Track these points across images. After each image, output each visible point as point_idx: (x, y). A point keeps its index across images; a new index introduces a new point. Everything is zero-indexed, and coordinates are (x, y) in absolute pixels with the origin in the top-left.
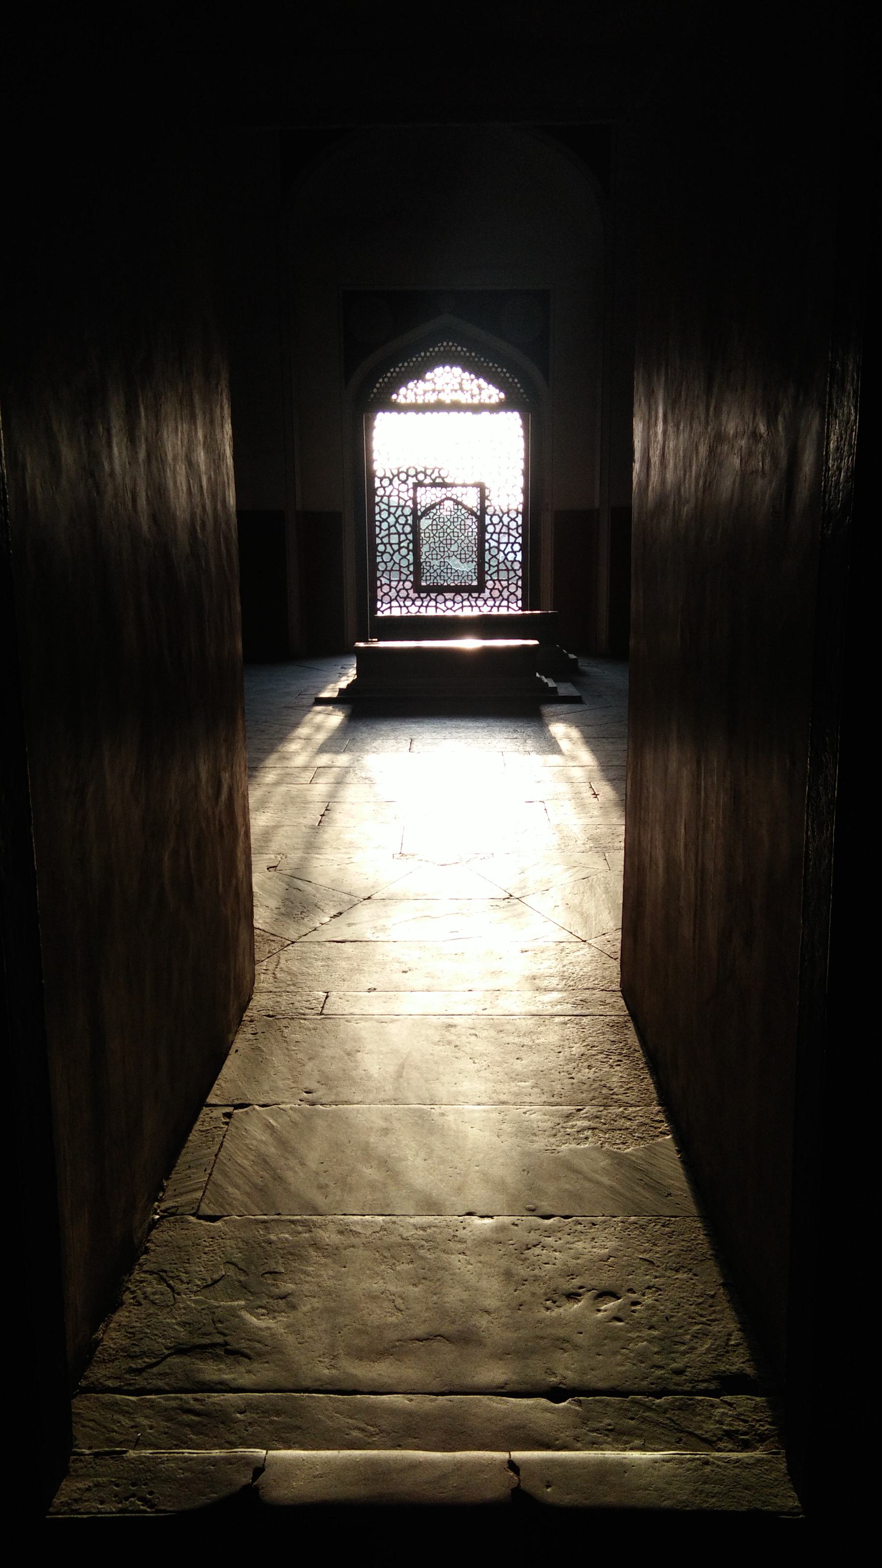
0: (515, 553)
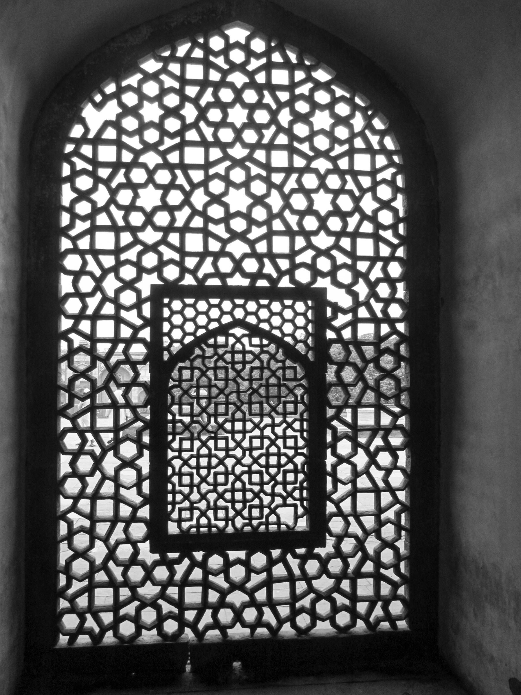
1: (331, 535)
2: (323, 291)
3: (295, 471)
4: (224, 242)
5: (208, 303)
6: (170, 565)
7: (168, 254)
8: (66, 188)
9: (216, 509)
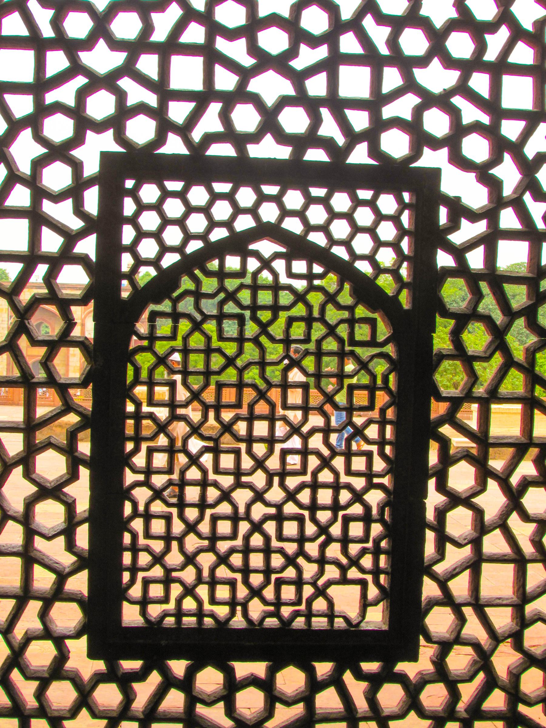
1: (429, 639)
2: (434, 175)
3: (367, 519)
4: (245, 74)
5: (210, 190)
6: (125, 682)
7: (137, 93)
9: (213, 583)
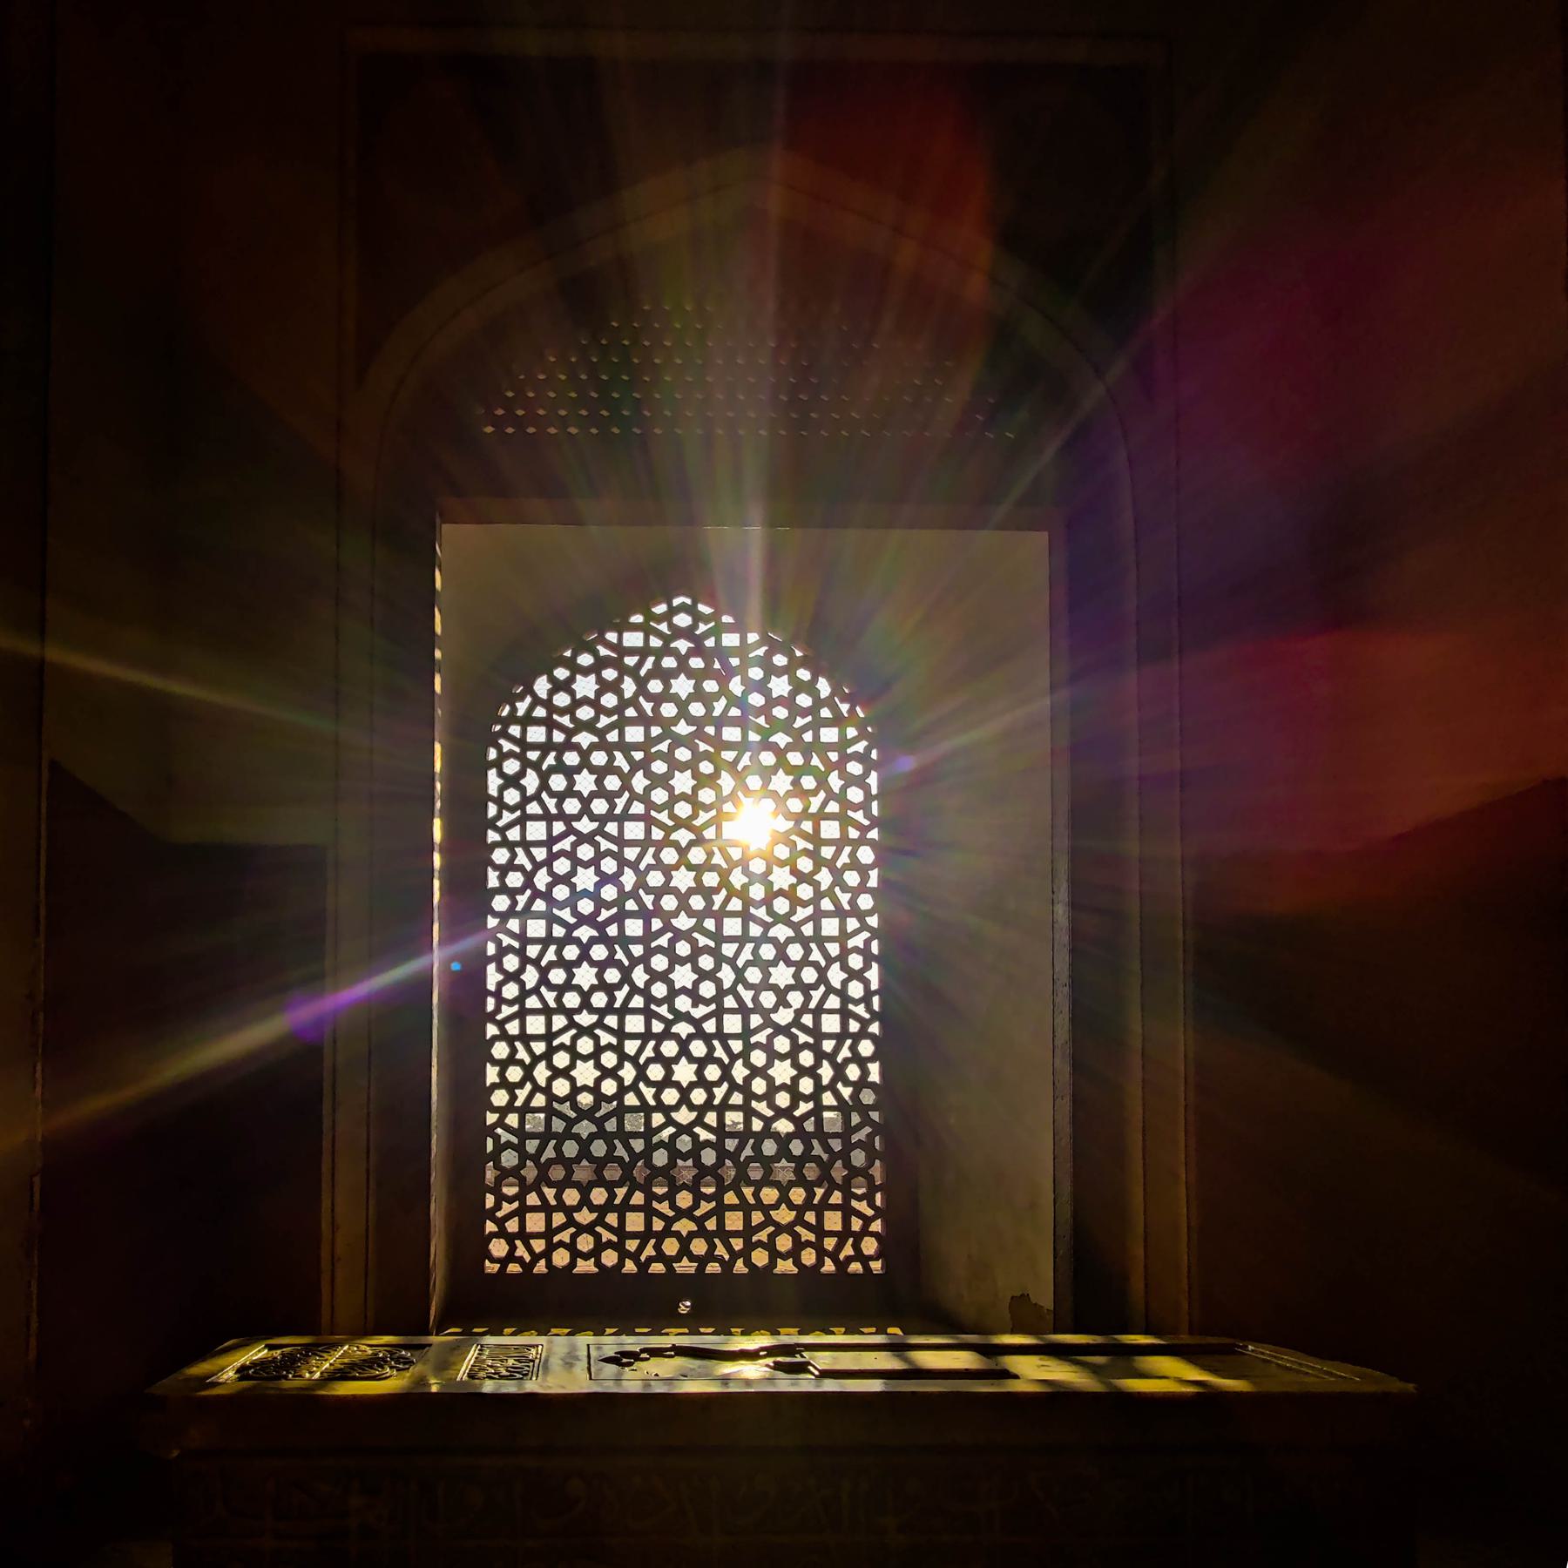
0: (862, 1062)
8: (492, 774)
